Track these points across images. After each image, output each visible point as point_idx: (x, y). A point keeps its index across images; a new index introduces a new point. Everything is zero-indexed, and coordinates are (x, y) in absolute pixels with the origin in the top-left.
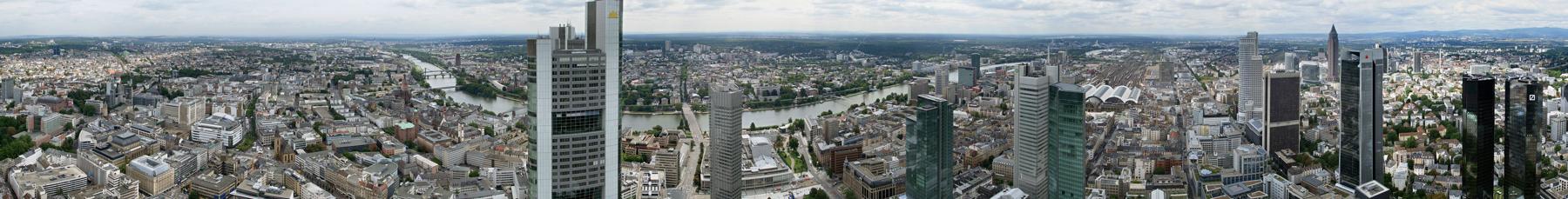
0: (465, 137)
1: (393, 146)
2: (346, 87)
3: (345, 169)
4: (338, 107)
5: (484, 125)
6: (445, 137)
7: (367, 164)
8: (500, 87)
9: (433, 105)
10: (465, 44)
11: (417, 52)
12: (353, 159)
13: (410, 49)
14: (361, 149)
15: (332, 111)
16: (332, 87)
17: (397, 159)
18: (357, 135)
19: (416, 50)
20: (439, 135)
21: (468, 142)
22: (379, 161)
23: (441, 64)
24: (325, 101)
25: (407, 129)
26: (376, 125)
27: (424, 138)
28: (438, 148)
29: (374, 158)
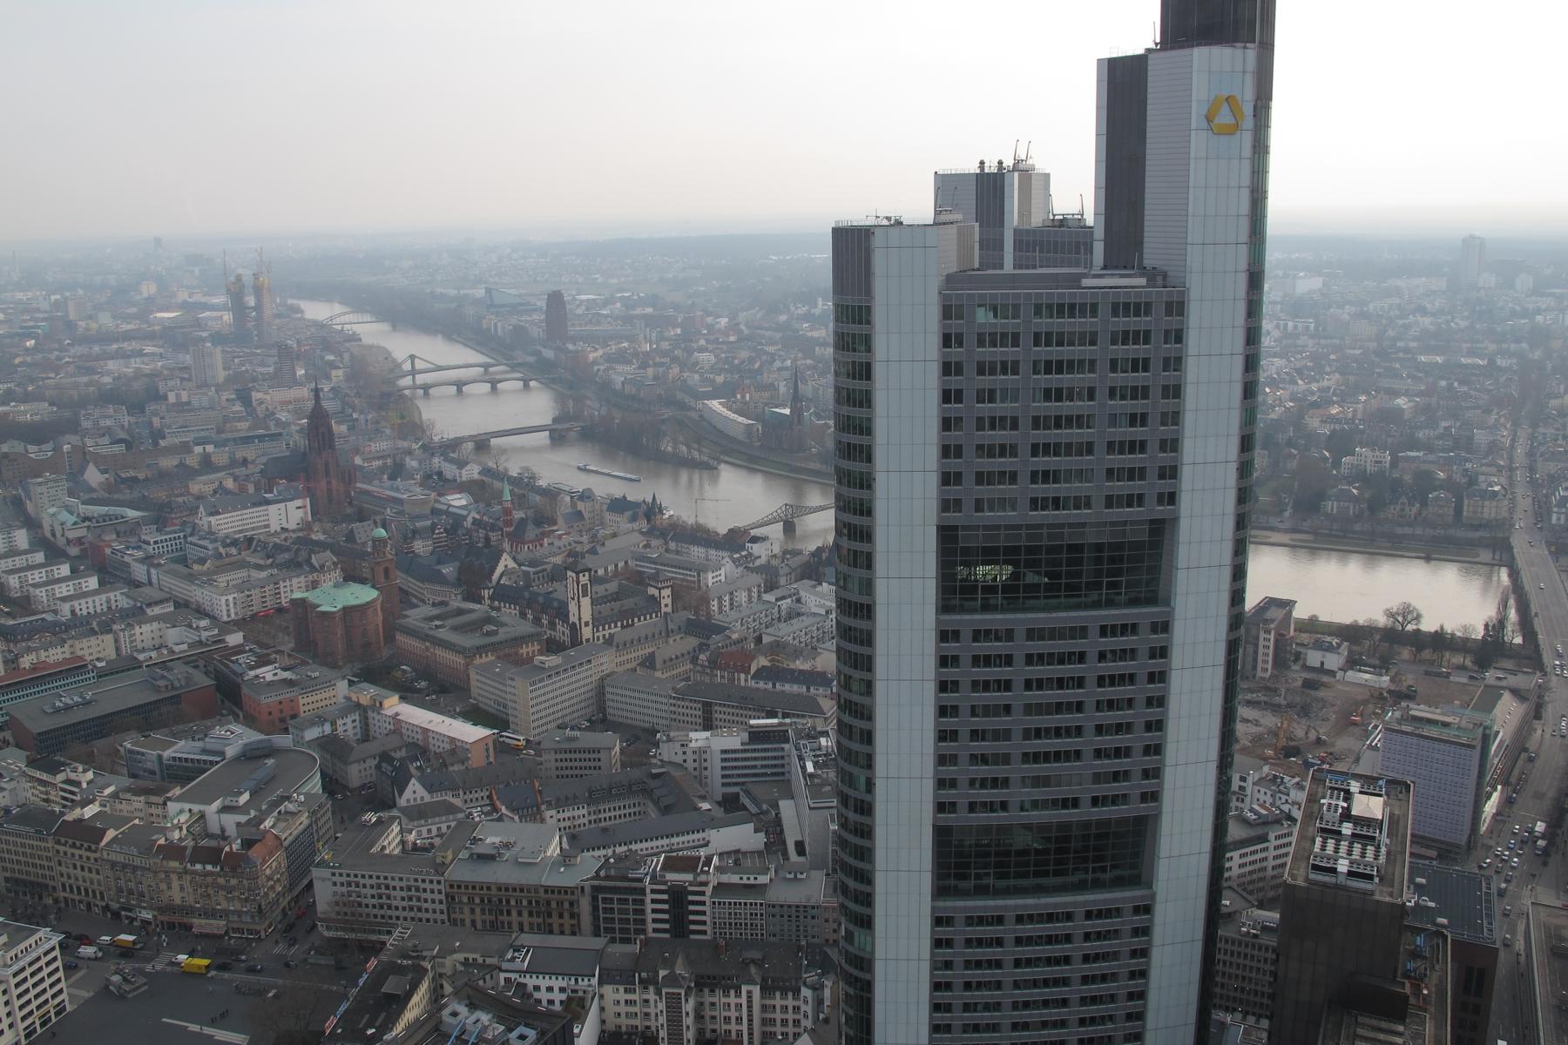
0: (597, 622)
1: (289, 683)
3: (90, 811)
4: (19, 562)
5: (670, 573)
6: (512, 620)
7: (181, 773)
9: (458, 501)
12: (105, 764)
14: (146, 718)
17: (312, 734)
18: (125, 665)
20: (488, 620)
21: (609, 641)
22: (231, 752)
25: (347, 610)
26: (201, 612)
27: (426, 638)
29: (210, 743)
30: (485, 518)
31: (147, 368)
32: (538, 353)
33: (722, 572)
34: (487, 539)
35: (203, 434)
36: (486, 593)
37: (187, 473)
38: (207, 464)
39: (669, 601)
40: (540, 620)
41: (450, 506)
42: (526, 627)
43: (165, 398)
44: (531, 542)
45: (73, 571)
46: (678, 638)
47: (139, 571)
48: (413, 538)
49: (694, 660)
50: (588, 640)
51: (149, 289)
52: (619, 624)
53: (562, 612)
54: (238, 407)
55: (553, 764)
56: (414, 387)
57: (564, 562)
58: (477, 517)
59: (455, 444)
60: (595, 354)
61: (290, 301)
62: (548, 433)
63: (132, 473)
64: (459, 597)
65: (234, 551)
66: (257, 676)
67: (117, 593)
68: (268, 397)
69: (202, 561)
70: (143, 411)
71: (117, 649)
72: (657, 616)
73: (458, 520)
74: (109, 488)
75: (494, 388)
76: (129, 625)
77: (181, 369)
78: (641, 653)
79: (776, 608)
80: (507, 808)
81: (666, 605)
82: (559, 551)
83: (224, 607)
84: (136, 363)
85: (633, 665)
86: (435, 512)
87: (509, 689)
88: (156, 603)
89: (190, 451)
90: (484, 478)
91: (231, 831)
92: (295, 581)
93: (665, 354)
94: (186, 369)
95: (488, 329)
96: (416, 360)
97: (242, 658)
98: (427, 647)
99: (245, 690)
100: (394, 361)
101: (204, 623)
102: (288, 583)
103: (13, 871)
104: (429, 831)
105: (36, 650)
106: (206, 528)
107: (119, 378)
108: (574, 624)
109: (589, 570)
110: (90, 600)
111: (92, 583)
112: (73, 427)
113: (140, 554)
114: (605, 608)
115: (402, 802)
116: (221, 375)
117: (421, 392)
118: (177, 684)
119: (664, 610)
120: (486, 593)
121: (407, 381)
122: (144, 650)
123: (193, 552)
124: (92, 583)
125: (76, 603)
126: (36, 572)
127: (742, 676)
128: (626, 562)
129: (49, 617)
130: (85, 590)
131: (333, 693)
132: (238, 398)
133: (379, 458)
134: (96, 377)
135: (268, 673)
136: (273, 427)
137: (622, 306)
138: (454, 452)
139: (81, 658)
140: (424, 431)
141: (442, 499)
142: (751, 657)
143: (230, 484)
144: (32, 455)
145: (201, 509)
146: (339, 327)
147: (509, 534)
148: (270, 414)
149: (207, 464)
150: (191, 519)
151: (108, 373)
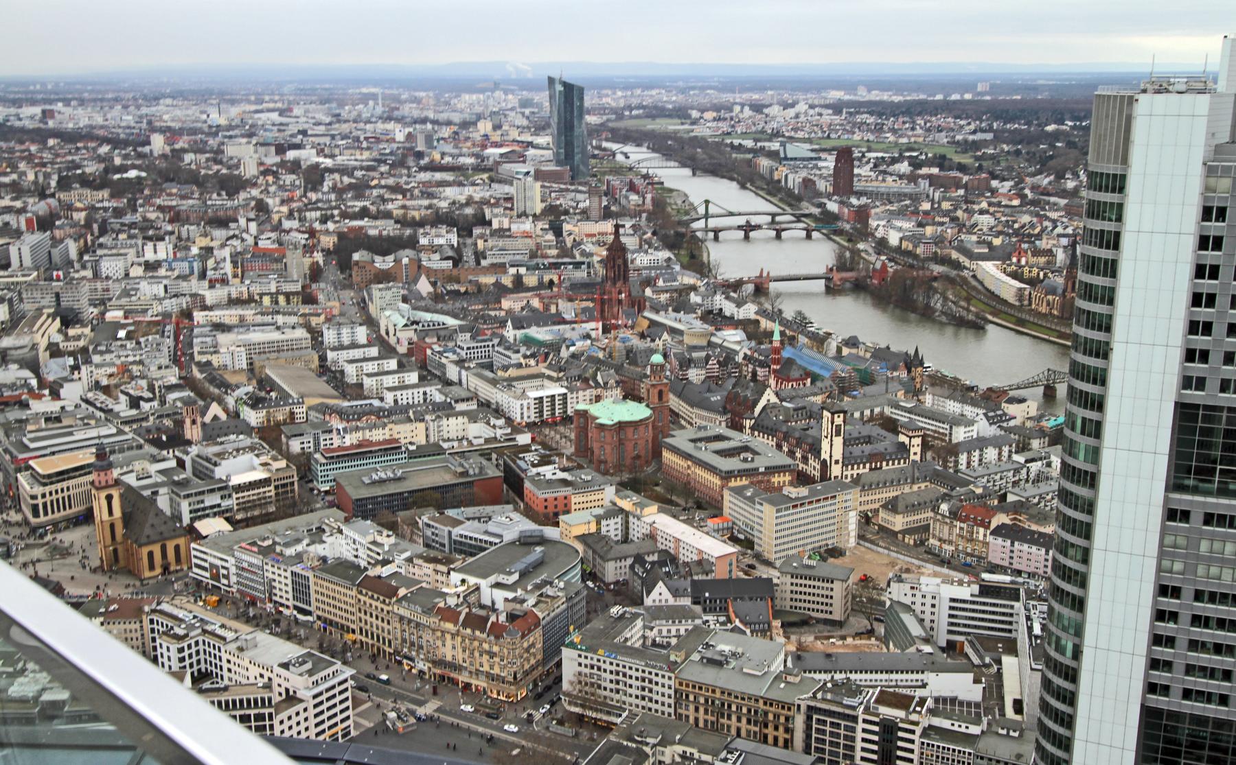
0: (848, 461)
1: (565, 482)
2: (384, 277)
3: (385, 571)
4: (357, 353)
6: (768, 453)
7: (468, 548)
8: (1008, 288)
9: (732, 338)
10: (882, 110)
11: (674, 136)
15: (334, 377)
16: (333, 273)
18: (431, 450)
19: (673, 126)
20: (746, 449)
21: (856, 481)
22: (509, 536)
23: (772, 188)
24: (301, 333)
25: (621, 426)
26: (498, 412)
27: (687, 456)
28: (739, 491)
29: (491, 527)
30: (756, 355)
31: (477, 197)
32: (822, 205)
33: (975, 428)
34: (754, 374)
35: (518, 257)
36: (748, 423)
37: (501, 291)
38: (519, 285)
39: (918, 450)
42: (782, 459)
43: (490, 223)
44: (796, 380)
45: (402, 367)
47: (452, 372)
48: (688, 367)
49: (935, 509)
50: (836, 477)
51: (485, 127)
52: (868, 465)
53: (816, 450)
54: (550, 236)
55: (789, 588)
56: (706, 230)
57: (824, 402)
58: (749, 353)
59: (737, 285)
61: (605, 144)
62: (823, 281)
63: (456, 287)
64: (724, 424)
65: (532, 362)
66: (538, 474)
67: (433, 388)
68: (576, 229)
69: (505, 368)
70: (470, 234)
71: (427, 436)
74: (437, 297)
75: (778, 237)
76: (438, 417)
77: (505, 199)
78: (885, 495)
79: (1024, 471)
80: (741, 621)
83: (519, 412)
84: (468, 191)
85: (876, 506)
86: (710, 345)
87: (756, 513)
88: (463, 400)
89: (505, 272)
90: (758, 318)
91: (500, 605)
92: (581, 393)
93: (946, 213)
94: (509, 199)
95: (779, 181)
96: (710, 205)
97: (531, 457)
99: (527, 484)
100: (691, 204)
101: (501, 422)
102: (574, 395)
103: (324, 610)
104: (669, 631)
105: (363, 429)
106: (511, 340)
107: (454, 203)
108: (825, 461)
109: (845, 412)
110: (410, 392)
111: (413, 377)
112: (412, 243)
113: (455, 357)
114: (857, 450)
115: (648, 601)
116: (539, 207)
117: (711, 235)
118: (471, 472)
119: (912, 457)
120: (748, 423)
121: (700, 224)
122: (449, 440)
123: (498, 360)
124: (413, 377)
125: (398, 393)
126: (370, 363)
127: (982, 530)
129: (376, 403)
130: (407, 383)
131: (600, 497)
132: (551, 228)
133: (667, 291)
134: (435, 201)
135: (548, 471)
136: (578, 256)
138: (735, 291)
139: (397, 441)
140: (710, 271)
141: (718, 333)
142: (993, 511)
143: (536, 303)
144: (377, 265)
145: (509, 323)
146: (644, 171)
147: (775, 371)
148: (576, 244)
149: (519, 285)
150: (500, 331)
151: (445, 199)
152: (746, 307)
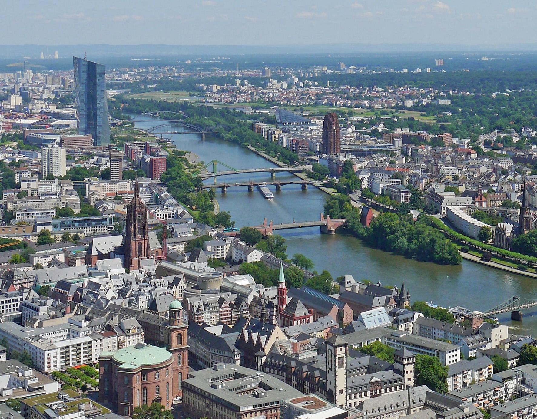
13: (161, 96)
39: (412, 376)
40: (302, 386)
41: (235, 285)
46: (418, 409)
52: (369, 393)
60: (361, 165)
72: (401, 388)
73: (241, 298)
81: (409, 379)
82: (322, 327)
92: (105, 340)
98: (207, 404)
102: (99, 343)
108: (330, 391)
119: (407, 383)
128: (377, 339)
137: (385, 126)
152: (253, 253)
